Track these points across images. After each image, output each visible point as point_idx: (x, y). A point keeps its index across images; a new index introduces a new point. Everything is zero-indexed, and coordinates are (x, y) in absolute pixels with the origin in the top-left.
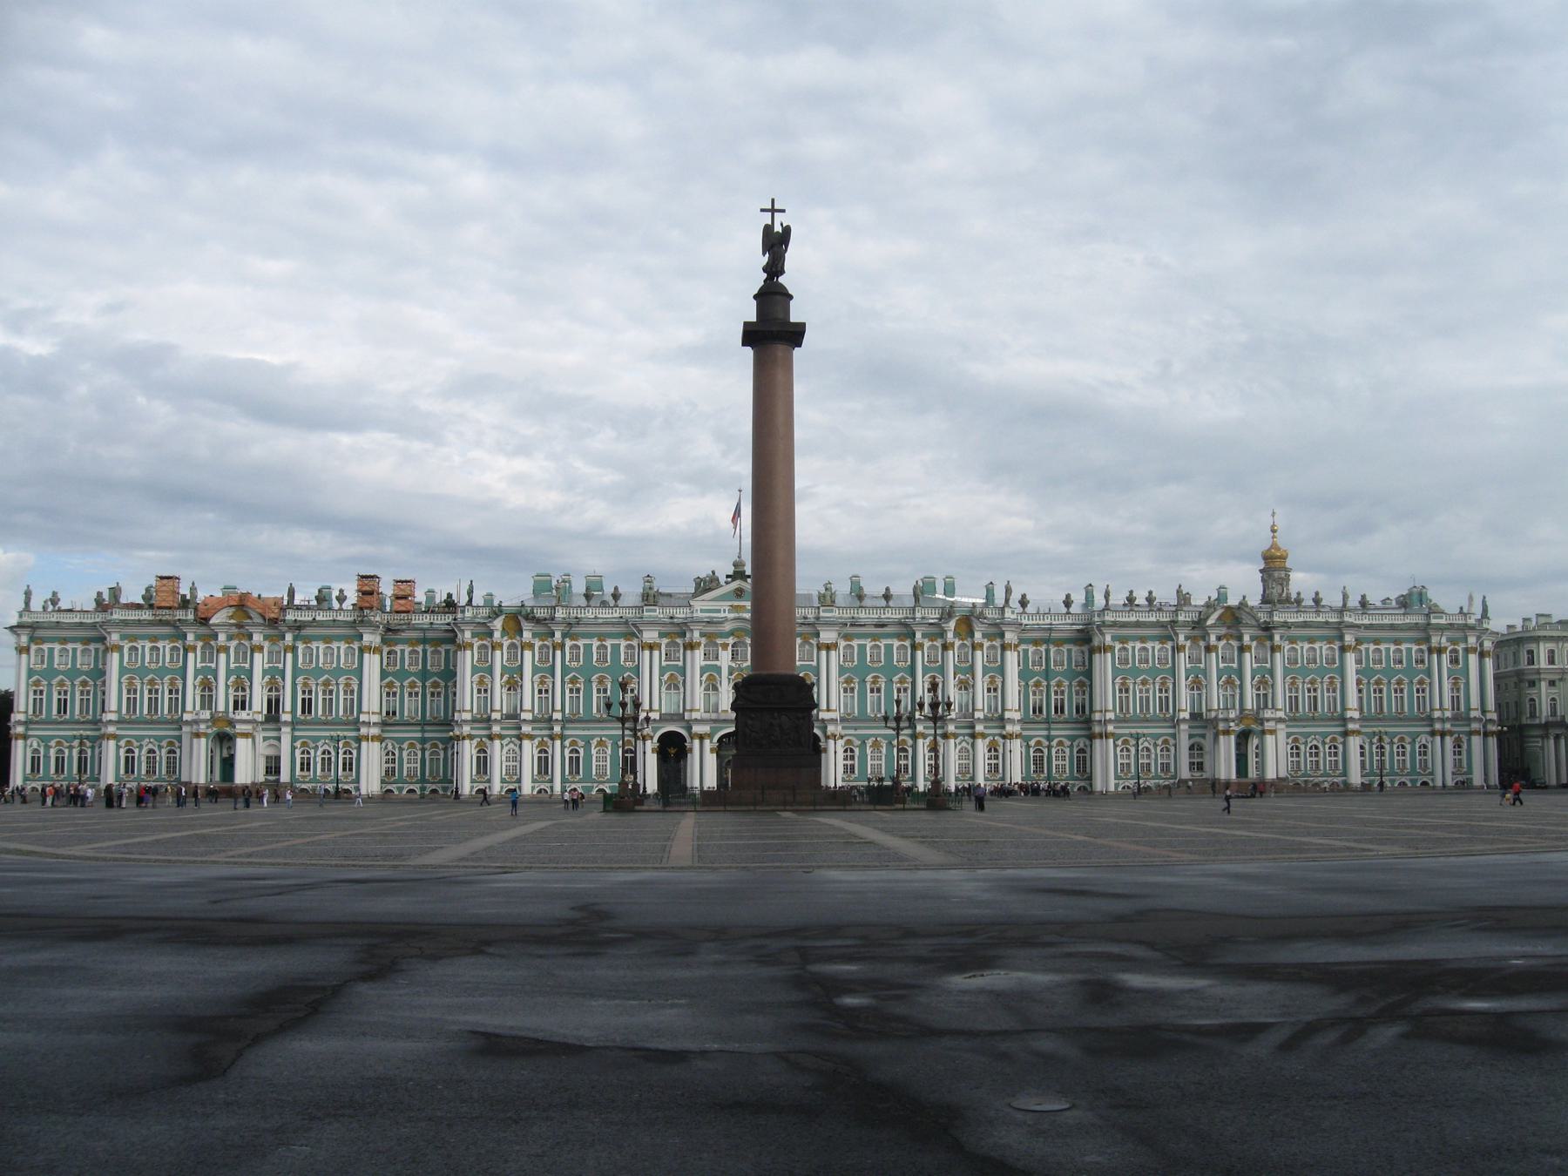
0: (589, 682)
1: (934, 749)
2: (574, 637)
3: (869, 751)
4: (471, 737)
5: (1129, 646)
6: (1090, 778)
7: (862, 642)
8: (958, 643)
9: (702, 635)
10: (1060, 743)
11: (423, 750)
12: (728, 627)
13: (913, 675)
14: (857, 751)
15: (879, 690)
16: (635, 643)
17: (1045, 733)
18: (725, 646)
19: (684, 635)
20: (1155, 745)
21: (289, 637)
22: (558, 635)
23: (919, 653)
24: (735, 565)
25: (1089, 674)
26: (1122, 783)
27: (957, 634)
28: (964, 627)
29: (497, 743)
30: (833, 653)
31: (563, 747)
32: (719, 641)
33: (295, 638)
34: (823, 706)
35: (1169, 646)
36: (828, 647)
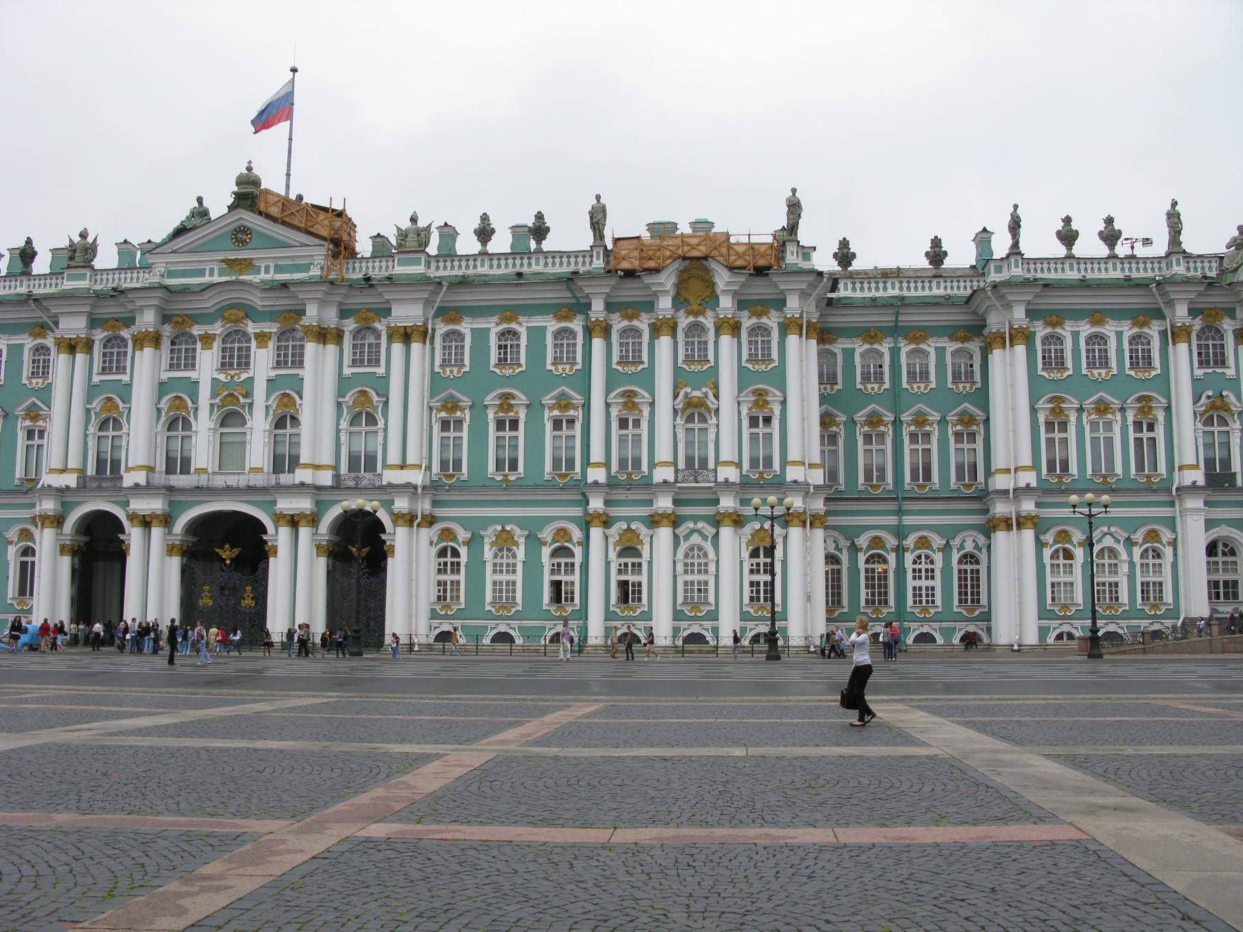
1: (629, 550)
3: (488, 554)
5: (1066, 332)
6: (987, 617)
7: (480, 324)
8: (684, 321)
9: (165, 318)
10: (923, 542)
12: (209, 303)
14: (463, 551)
15: (514, 424)
16: (49, 342)
17: (892, 520)
18: (207, 340)
19: (129, 321)
20: (1129, 543)
23: (598, 344)
24: (239, 182)
25: (982, 397)
26: (1056, 627)
27: (678, 301)
28: (696, 286)
30: (416, 347)
32: (196, 331)
34: (394, 457)
36: (406, 336)
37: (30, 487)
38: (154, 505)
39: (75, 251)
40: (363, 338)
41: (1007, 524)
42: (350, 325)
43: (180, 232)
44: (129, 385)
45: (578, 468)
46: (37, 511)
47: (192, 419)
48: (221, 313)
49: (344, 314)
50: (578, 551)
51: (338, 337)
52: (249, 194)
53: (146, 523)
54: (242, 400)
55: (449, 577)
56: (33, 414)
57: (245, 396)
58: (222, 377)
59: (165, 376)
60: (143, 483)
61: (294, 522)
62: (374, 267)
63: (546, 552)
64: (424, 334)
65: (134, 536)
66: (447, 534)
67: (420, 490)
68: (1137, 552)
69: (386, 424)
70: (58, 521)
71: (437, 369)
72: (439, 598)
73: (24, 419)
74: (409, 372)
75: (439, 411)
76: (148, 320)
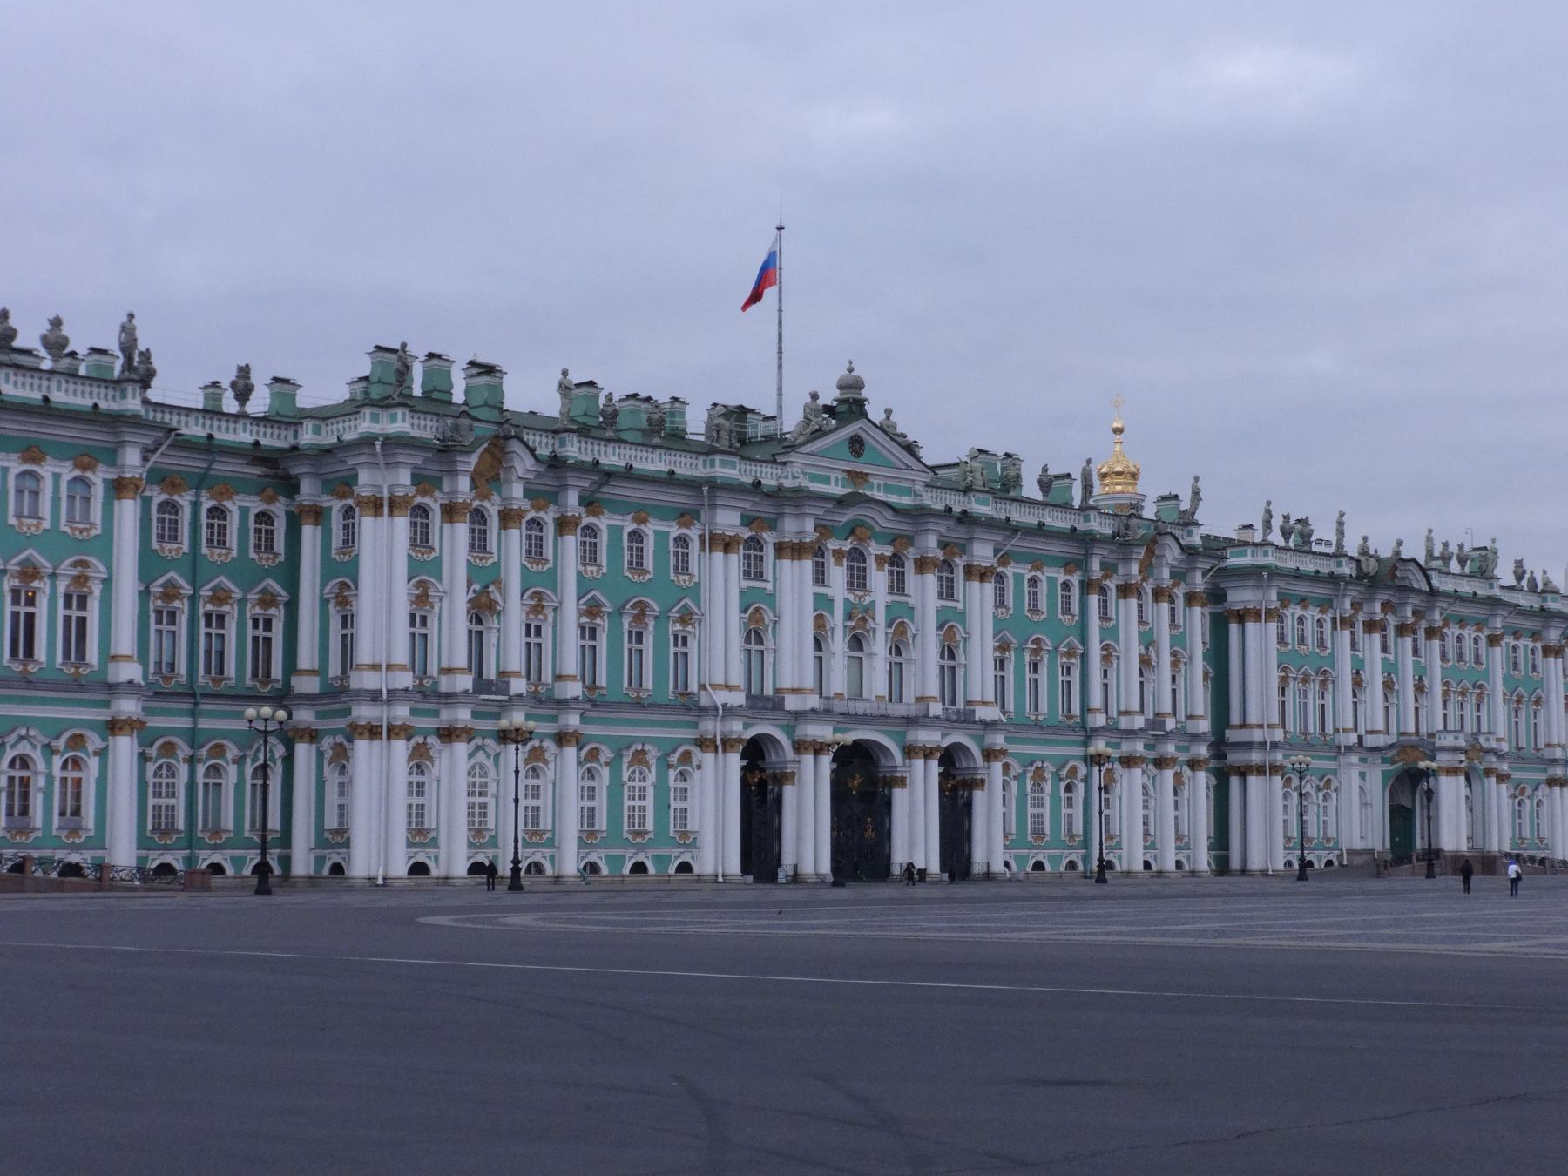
4: (405, 732)
5: (1288, 613)
11: (192, 761)
13: (1084, 640)
14: (1014, 784)
16: (693, 533)
18: (838, 554)
20: (1318, 789)
29: (461, 748)
31: (579, 764)
32: (832, 544)
35: (1328, 618)
41: (1260, 770)
45: (1076, 710)
48: (852, 530)
50: (1081, 786)
54: (871, 624)
56: (686, 618)
58: (851, 597)
61: (928, 753)
63: (1063, 786)
68: (1321, 795)
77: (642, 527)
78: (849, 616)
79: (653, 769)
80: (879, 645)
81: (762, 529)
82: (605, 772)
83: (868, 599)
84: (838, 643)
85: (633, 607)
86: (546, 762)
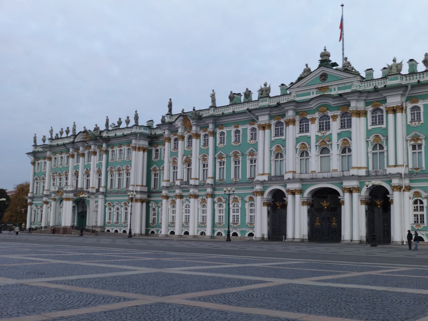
0: (228, 157)
2: (222, 126)
14: (425, 201)
16: (256, 126)
18: (313, 120)
21: (104, 145)
22: (211, 126)
24: (322, 56)
30: (399, 115)
31: (214, 203)
33: (108, 146)
34: (392, 163)
36: (394, 111)
37: (251, 182)
38: (296, 186)
39: (263, 91)
40: (376, 113)
42: (370, 109)
43: (300, 79)
44: (285, 140)
46: (254, 190)
47: (309, 152)
48: (318, 109)
49: (367, 104)
51: (365, 113)
52: (325, 61)
53: (293, 193)
54: (328, 143)
55: (419, 213)
56: (252, 154)
57: (329, 141)
58: (319, 134)
59: (298, 135)
60: (291, 178)
62: (378, 83)
64: (402, 109)
65: (289, 198)
66: (417, 194)
67: (403, 176)
69: (387, 149)
70: (262, 193)
71: (409, 123)
72: (415, 221)
73: (249, 156)
74: (397, 126)
75: (411, 141)
76: (290, 114)
77: (238, 129)
78: (317, 142)
79: (240, 203)
80: (335, 151)
81: (280, 119)
82: (224, 205)
83: (328, 133)
84: (314, 152)
85: (233, 153)
86: (206, 203)
